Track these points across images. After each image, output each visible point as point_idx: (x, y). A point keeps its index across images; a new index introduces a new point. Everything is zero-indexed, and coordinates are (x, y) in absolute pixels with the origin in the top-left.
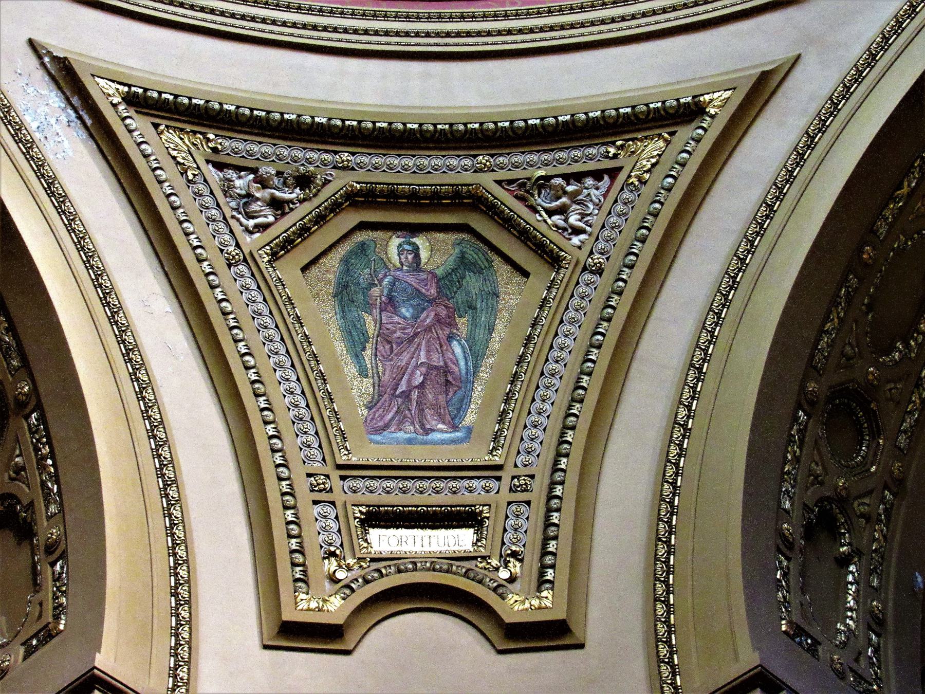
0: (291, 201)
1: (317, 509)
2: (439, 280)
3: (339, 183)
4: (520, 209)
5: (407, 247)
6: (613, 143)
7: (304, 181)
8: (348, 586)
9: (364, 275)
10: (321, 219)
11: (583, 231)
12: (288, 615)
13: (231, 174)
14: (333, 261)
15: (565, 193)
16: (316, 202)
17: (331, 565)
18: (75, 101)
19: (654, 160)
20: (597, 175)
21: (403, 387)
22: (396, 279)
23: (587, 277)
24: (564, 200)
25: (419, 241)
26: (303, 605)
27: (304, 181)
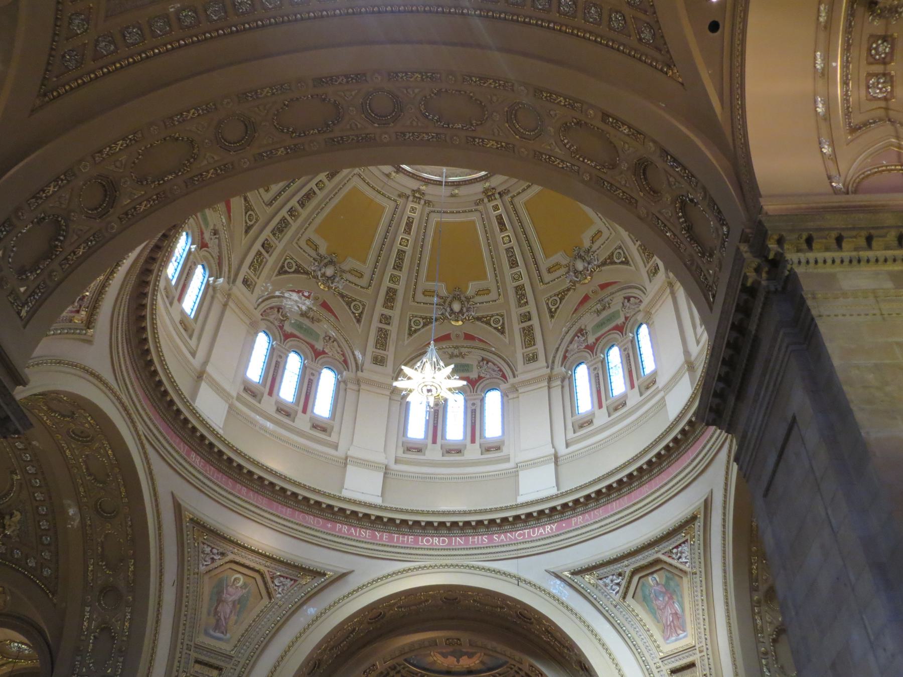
2: (664, 586)
3: (631, 568)
7: (620, 575)
10: (629, 582)
16: (626, 579)
20: (684, 543)
21: (669, 623)
23: (694, 576)
24: (679, 555)
25: (655, 576)
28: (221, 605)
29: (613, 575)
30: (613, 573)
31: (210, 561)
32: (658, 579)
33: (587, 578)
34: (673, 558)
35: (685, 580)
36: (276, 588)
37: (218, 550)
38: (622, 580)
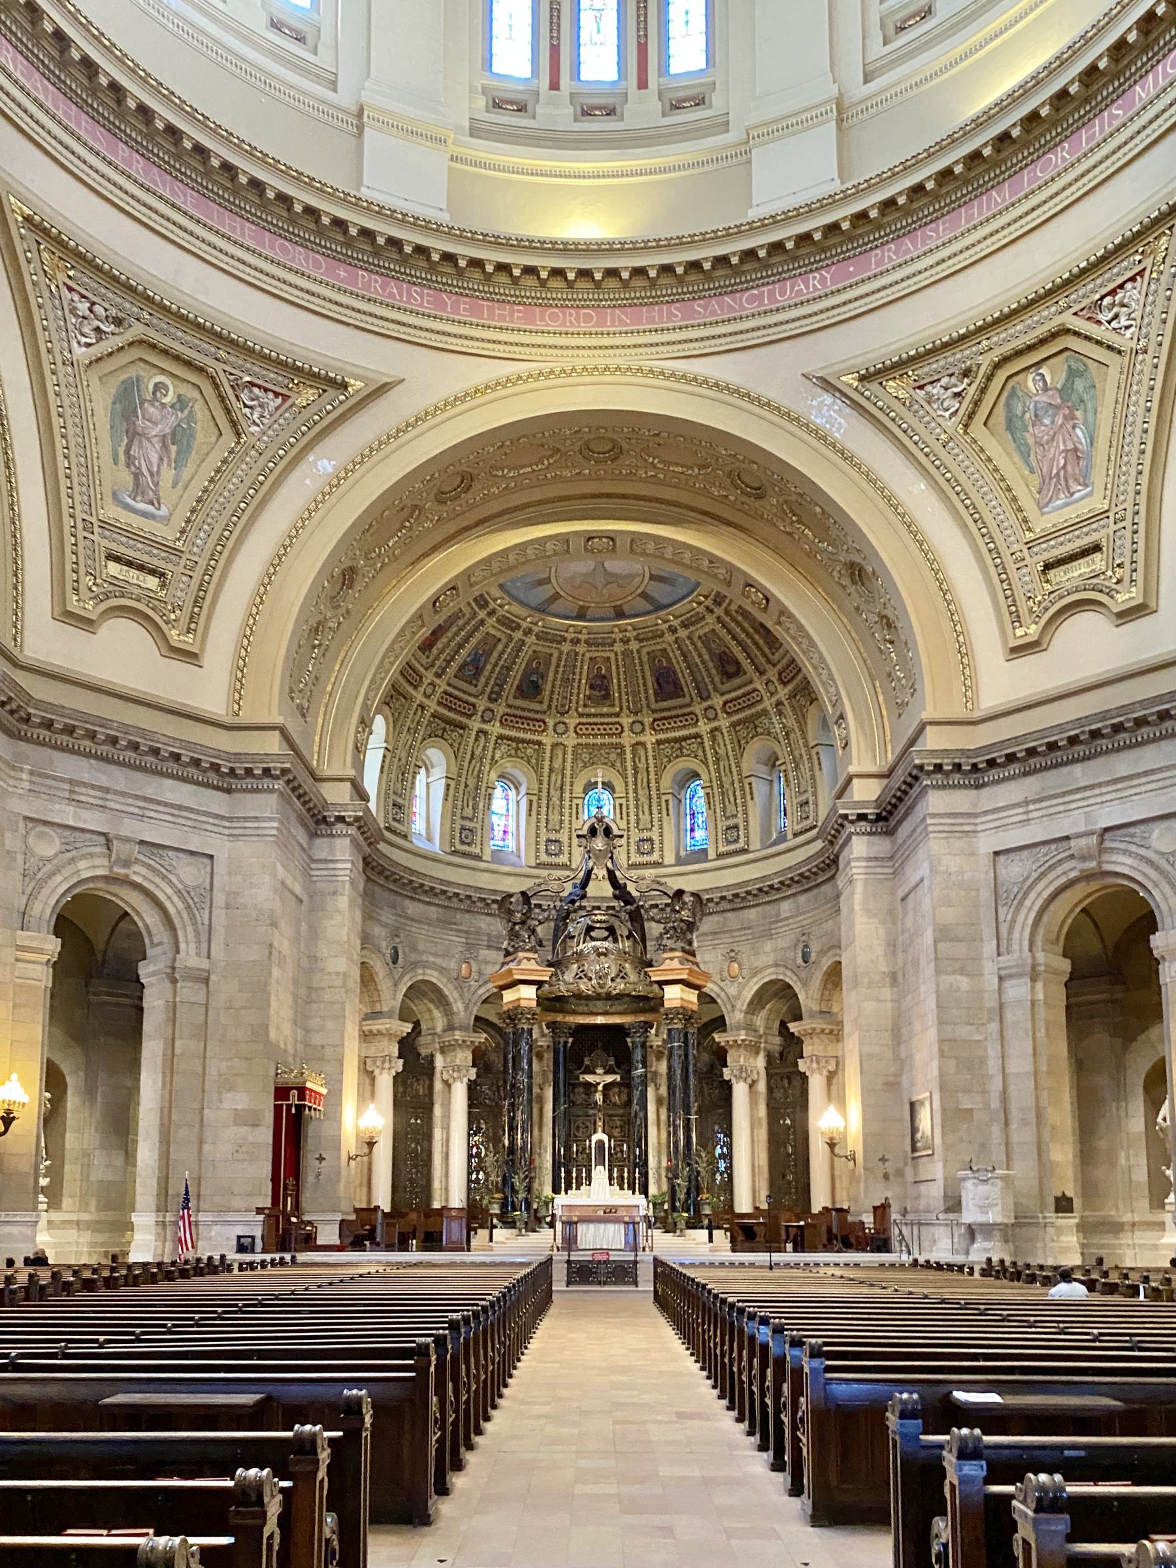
5: (1038, 378)
9: (1019, 410)
14: (1000, 409)
18: (837, 394)
21: (1055, 471)
22: (1036, 402)
28: (136, 443)
29: (950, 375)
30: (950, 372)
31: (93, 334)
32: (1048, 379)
33: (891, 387)
34: (1099, 322)
36: (247, 411)
37: (106, 310)
38: (969, 385)
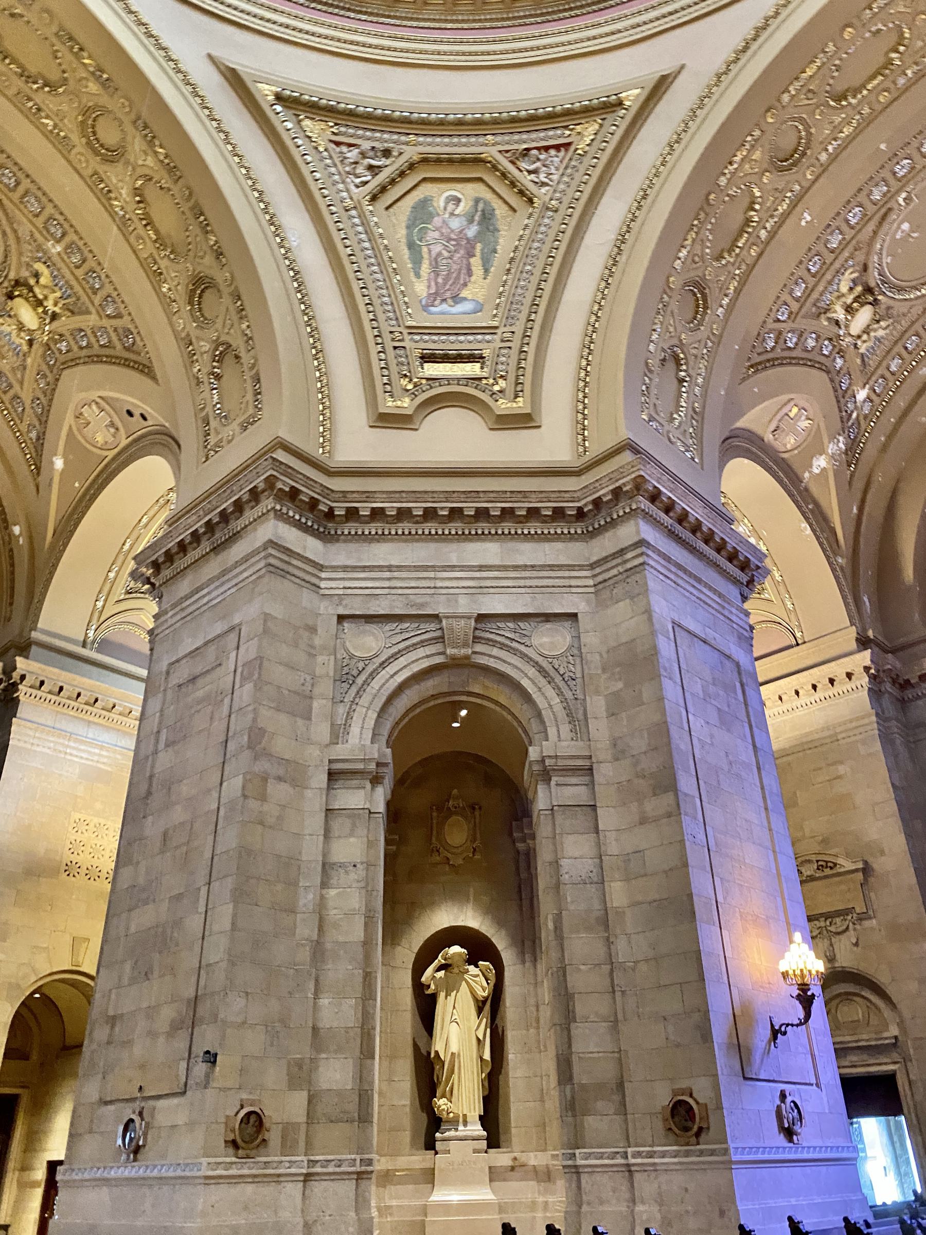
0: (379, 167)
1: (398, 351)
4: (511, 168)
6: (566, 127)
7: (387, 153)
8: (413, 393)
11: (547, 184)
12: (382, 410)
13: (344, 149)
15: (538, 159)
17: (404, 382)
19: (592, 137)
24: (538, 164)
26: (390, 404)
27: (387, 153)
35: (522, 218)
